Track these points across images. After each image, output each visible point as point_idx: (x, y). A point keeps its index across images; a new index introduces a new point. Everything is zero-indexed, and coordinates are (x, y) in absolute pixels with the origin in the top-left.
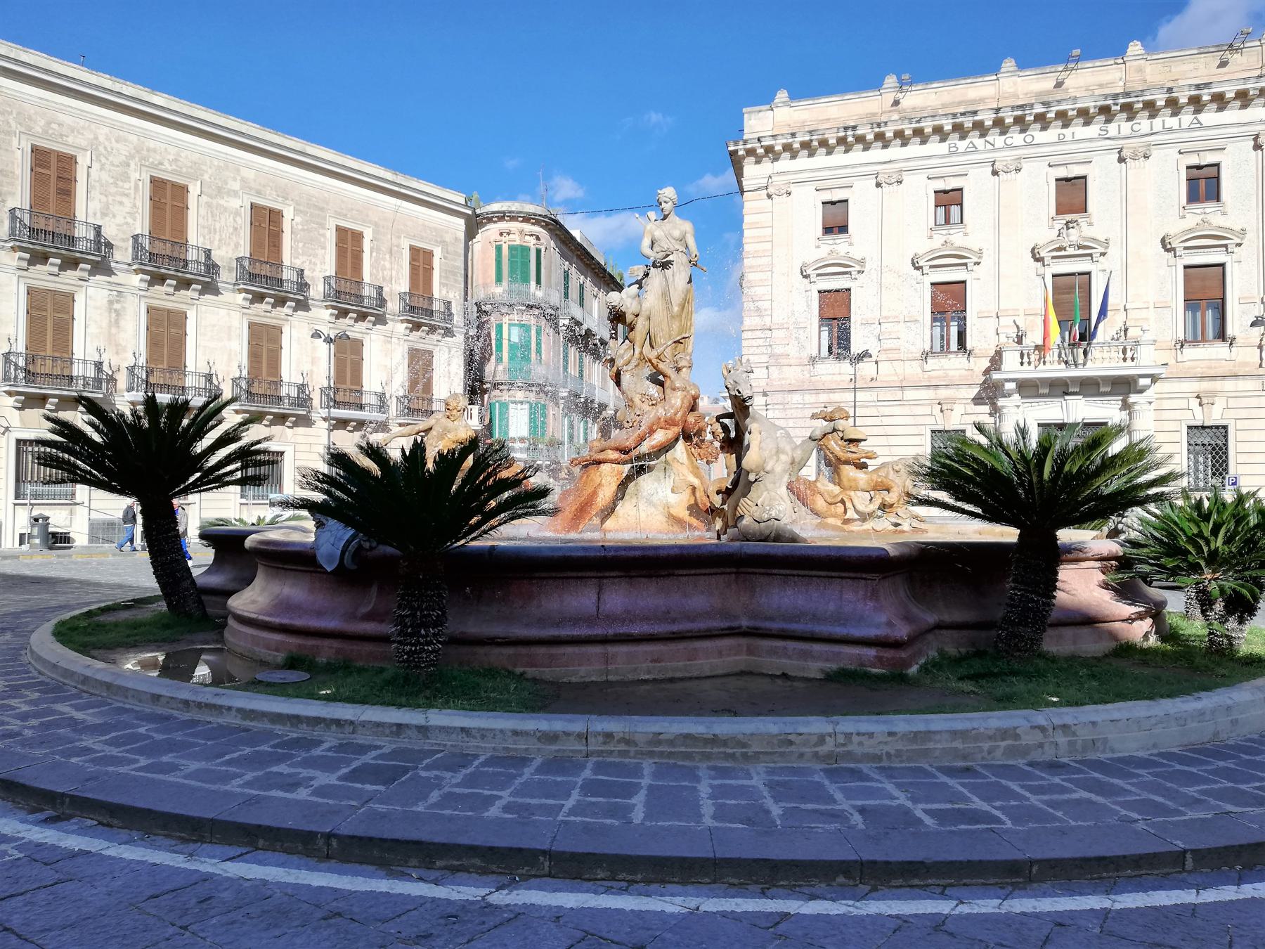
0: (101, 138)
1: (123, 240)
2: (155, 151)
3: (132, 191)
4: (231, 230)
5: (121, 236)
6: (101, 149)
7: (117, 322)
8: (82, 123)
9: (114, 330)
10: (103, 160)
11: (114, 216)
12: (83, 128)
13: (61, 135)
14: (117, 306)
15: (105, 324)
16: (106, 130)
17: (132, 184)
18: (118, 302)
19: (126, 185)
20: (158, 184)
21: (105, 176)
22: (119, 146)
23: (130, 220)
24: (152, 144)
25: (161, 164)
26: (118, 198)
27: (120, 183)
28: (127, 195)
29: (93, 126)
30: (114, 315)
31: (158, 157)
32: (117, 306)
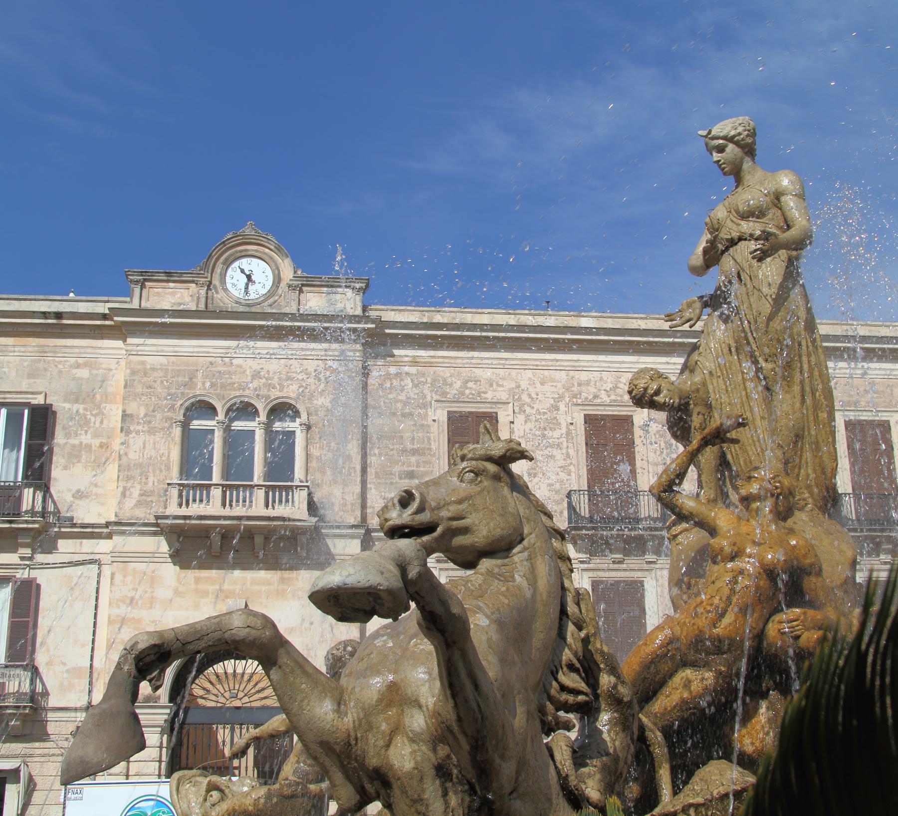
0: (524, 385)
1: (558, 503)
2: (588, 383)
8: (501, 372)
10: (528, 410)
12: (503, 379)
13: (479, 393)
16: (529, 374)
17: (564, 431)
19: (556, 434)
23: (563, 476)
24: (584, 376)
25: (595, 397)
28: (559, 446)
29: (514, 373)
31: (592, 390)
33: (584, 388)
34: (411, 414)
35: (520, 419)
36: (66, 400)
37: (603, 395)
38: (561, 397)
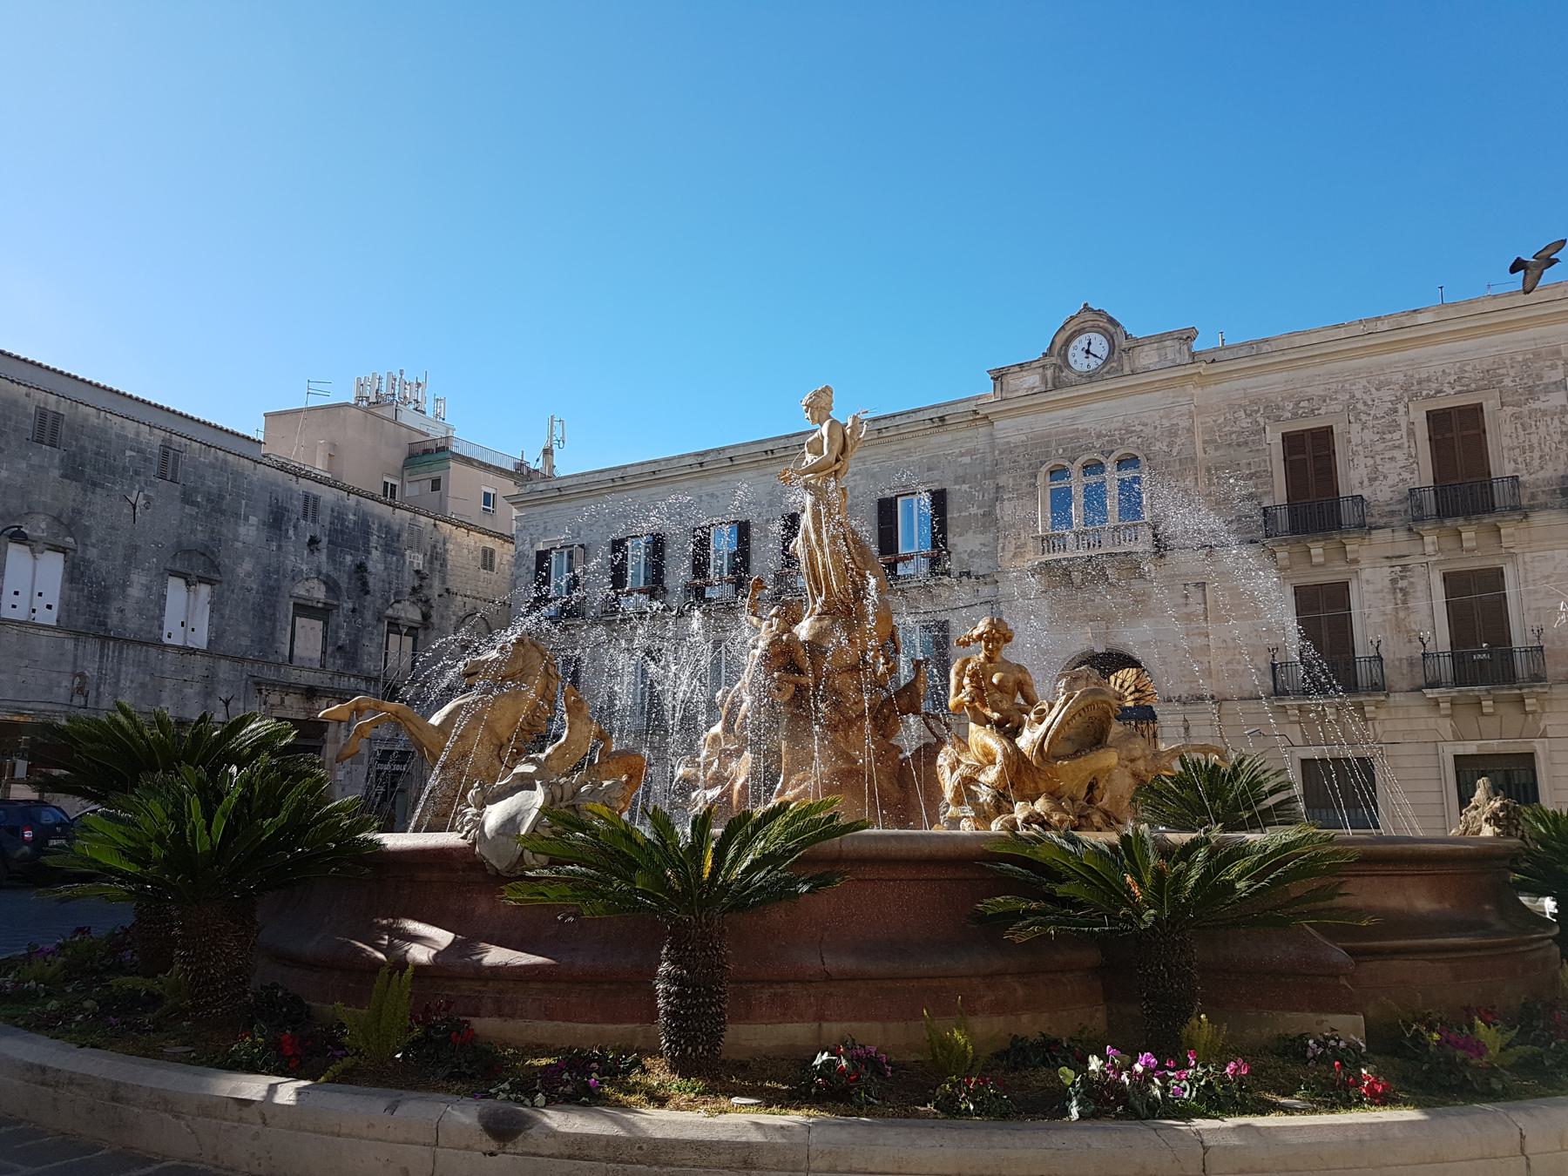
1: (1401, 502)
3: (1405, 439)
4: (1557, 438)
5: (1397, 497)
6: (1360, 406)
7: (1405, 602)
9: (1402, 615)
11: (1385, 477)
14: (1402, 584)
15: (1390, 607)
18: (1402, 578)
19: (1396, 436)
20: (1437, 420)
21: (1369, 435)
22: (1380, 393)
23: (1406, 475)
26: (1388, 455)
27: (1388, 436)
30: (1400, 595)
31: (1434, 386)
32: (1402, 584)
33: (1425, 385)
34: (1246, 443)
35: (1356, 427)
36: (956, 483)
37: (1447, 389)
38: (1399, 399)
